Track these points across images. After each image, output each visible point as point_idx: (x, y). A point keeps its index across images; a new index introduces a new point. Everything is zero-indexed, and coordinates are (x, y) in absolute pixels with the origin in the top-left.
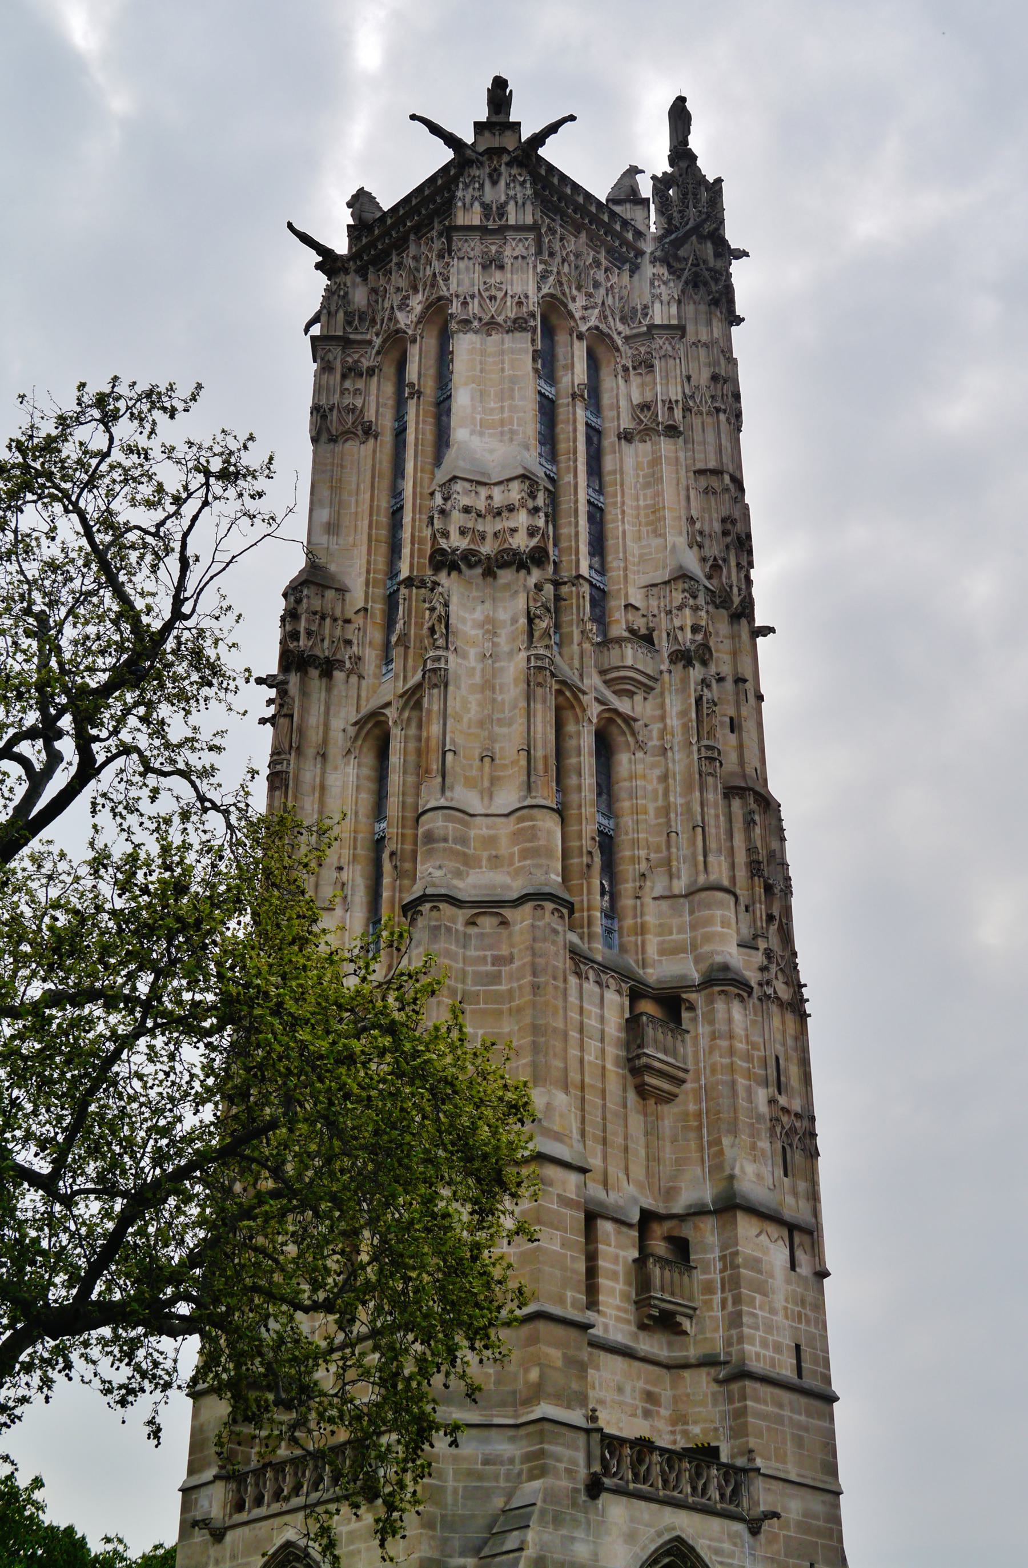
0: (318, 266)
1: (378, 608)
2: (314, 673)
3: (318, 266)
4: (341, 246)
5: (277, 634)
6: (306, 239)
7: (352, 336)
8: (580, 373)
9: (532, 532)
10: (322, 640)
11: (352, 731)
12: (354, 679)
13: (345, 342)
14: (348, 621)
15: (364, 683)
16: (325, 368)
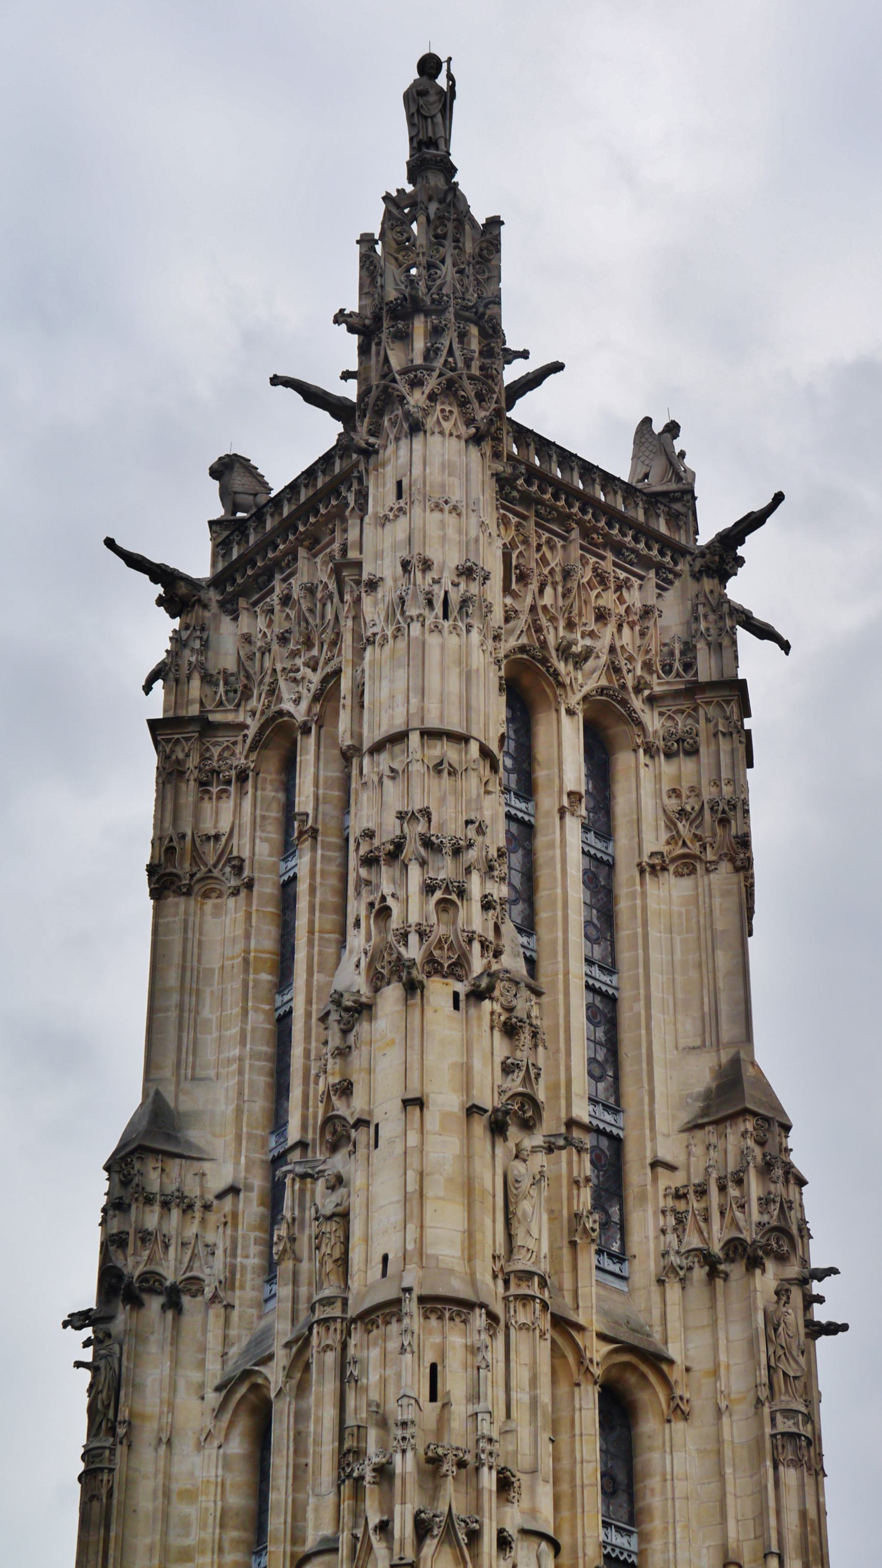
0: (160, 601)
1: (258, 1181)
2: (155, 1304)
3: (160, 601)
4: (197, 561)
5: (94, 1238)
6: (135, 562)
7: (212, 717)
8: (573, 772)
10: (166, 1246)
11: (213, 1398)
12: (217, 1310)
13: (205, 727)
14: (207, 1207)
15: (235, 1314)
16: (169, 775)
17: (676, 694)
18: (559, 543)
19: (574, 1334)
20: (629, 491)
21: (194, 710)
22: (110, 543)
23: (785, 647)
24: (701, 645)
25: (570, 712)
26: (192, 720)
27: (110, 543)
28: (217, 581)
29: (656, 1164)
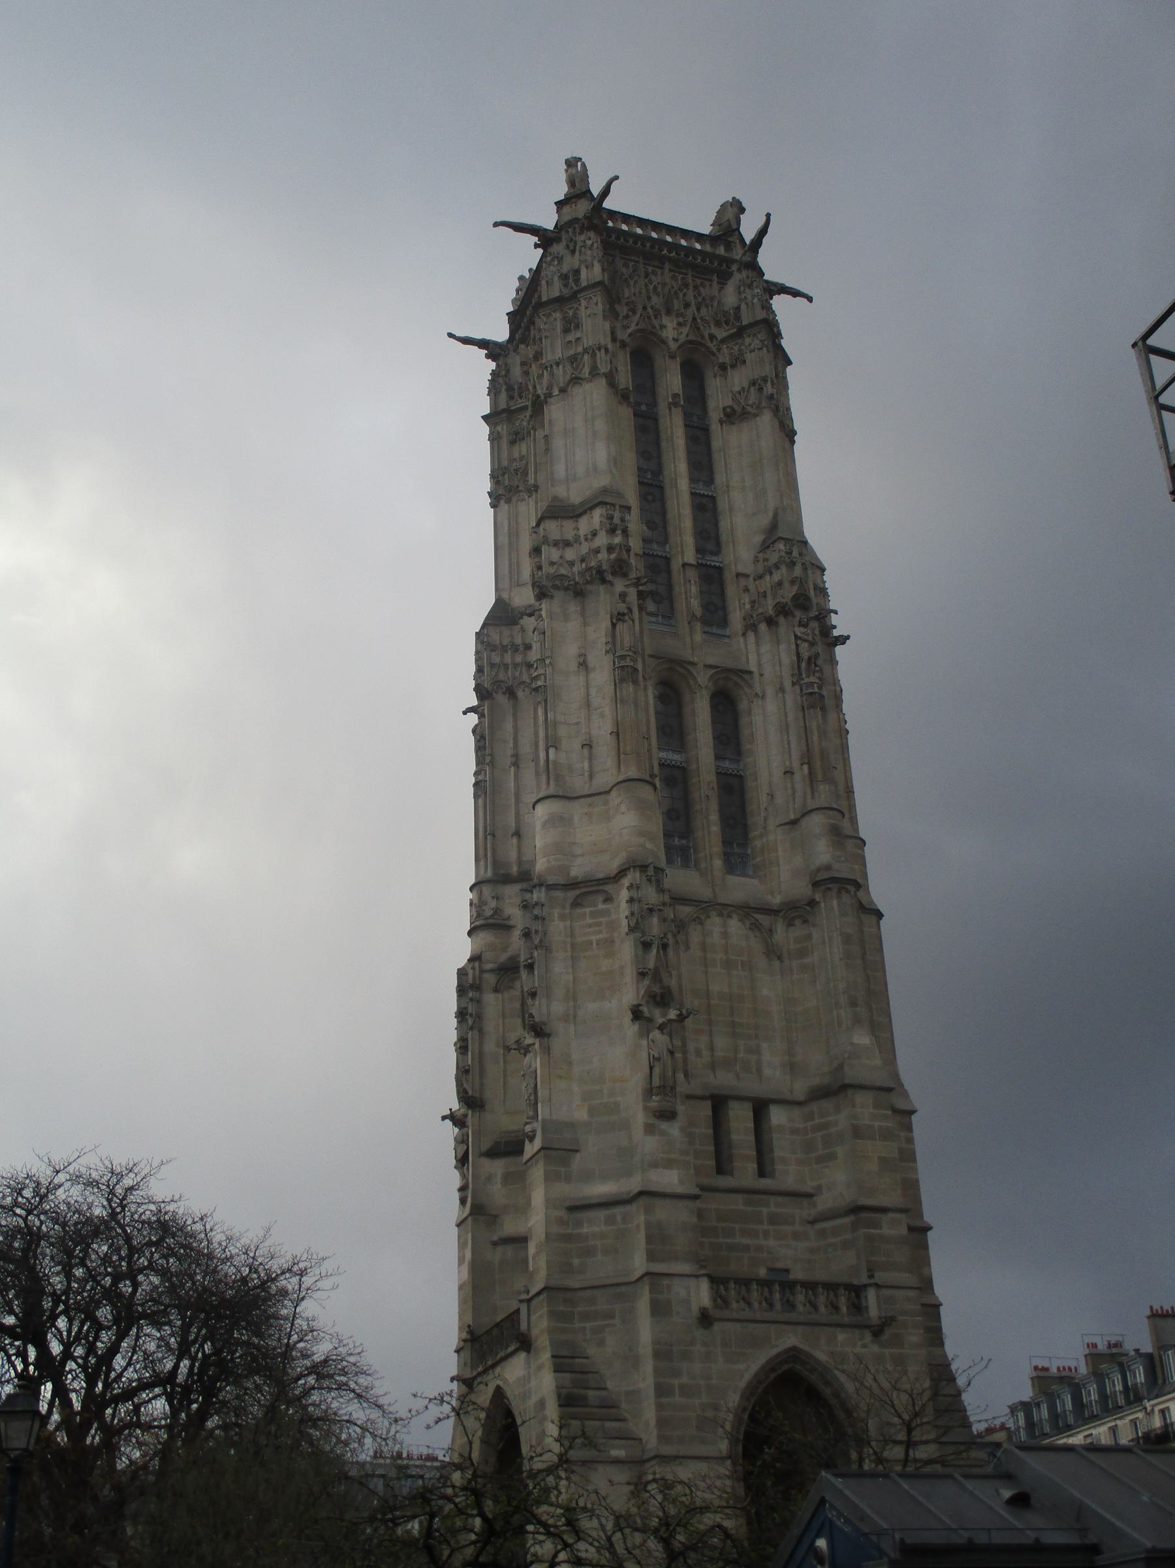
3: (488, 356)
4: (501, 333)
6: (466, 341)
9: (610, 549)
17: (731, 337)
18: (659, 271)
19: (690, 668)
20: (699, 237)
21: (503, 405)
22: (451, 335)
23: (810, 299)
24: (743, 306)
25: (672, 357)
26: (504, 411)
27: (451, 335)
28: (511, 339)
29: (738, 575)
